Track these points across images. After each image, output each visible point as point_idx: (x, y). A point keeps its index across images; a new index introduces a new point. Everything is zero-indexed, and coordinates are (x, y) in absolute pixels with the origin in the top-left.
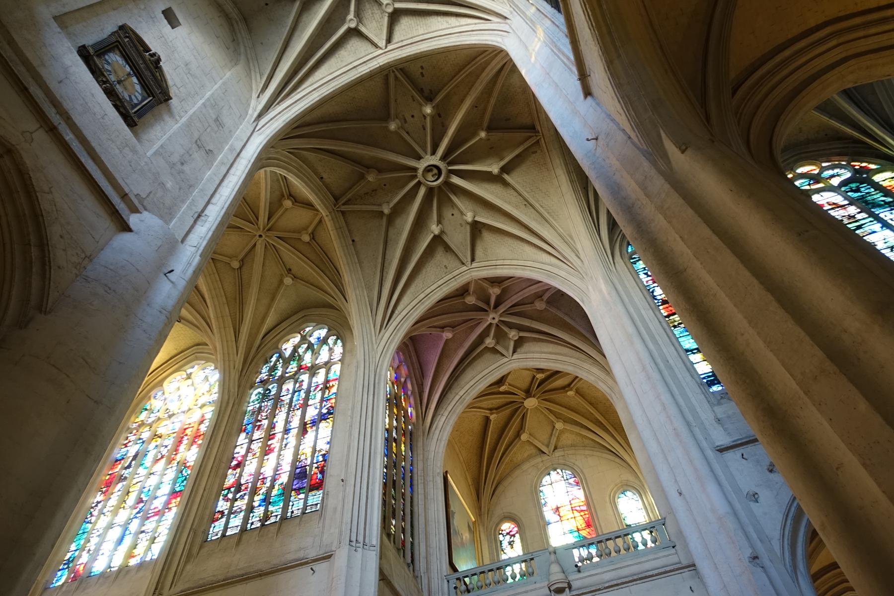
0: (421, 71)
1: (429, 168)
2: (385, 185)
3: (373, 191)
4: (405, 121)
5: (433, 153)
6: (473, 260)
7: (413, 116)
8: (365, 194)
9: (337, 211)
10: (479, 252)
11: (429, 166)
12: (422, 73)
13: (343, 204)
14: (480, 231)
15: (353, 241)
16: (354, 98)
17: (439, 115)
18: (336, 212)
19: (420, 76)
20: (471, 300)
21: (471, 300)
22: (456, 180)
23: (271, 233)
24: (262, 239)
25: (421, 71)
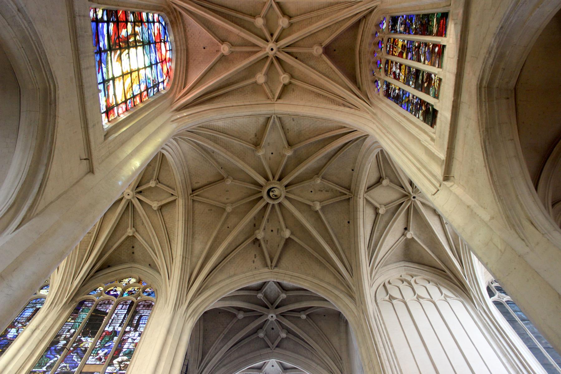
0: (255, 260)
1: (274, 198)
2: (311, 192)
3: (322, 191)
4: (278, 230)
5: (268, 203)
6: (268, 119)
7: (272, 231)
8: (328, 191)
9: (352, 194)
10: (262, 120)
11: (274, 199)
12: (255, 258)
13: (346, 194)
14: (256, 136)
15: (353, 170)
16: (301, 263)
17: (255, 225)
18: (353, 193)
19: (257, 255)
20: (284, 78)
21: (284, 78)
22: (261, 180)
23: (408, 194)
24: (415, 195)
25: (255, 260)
